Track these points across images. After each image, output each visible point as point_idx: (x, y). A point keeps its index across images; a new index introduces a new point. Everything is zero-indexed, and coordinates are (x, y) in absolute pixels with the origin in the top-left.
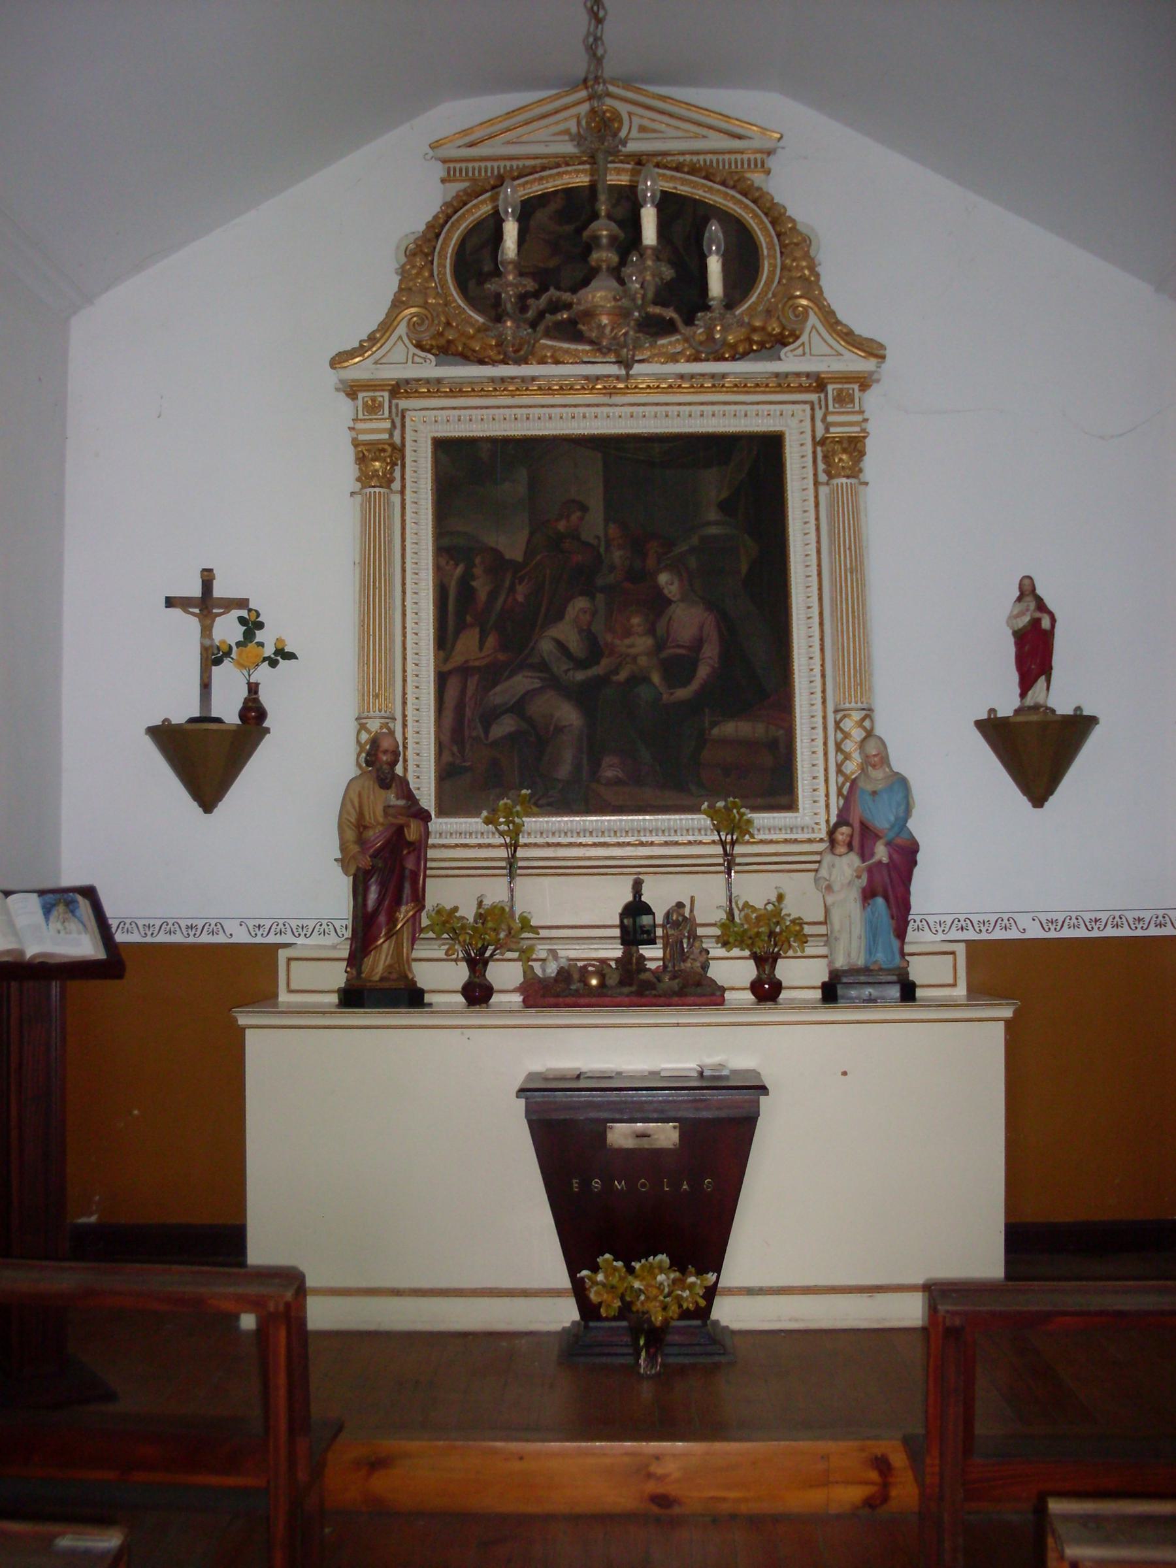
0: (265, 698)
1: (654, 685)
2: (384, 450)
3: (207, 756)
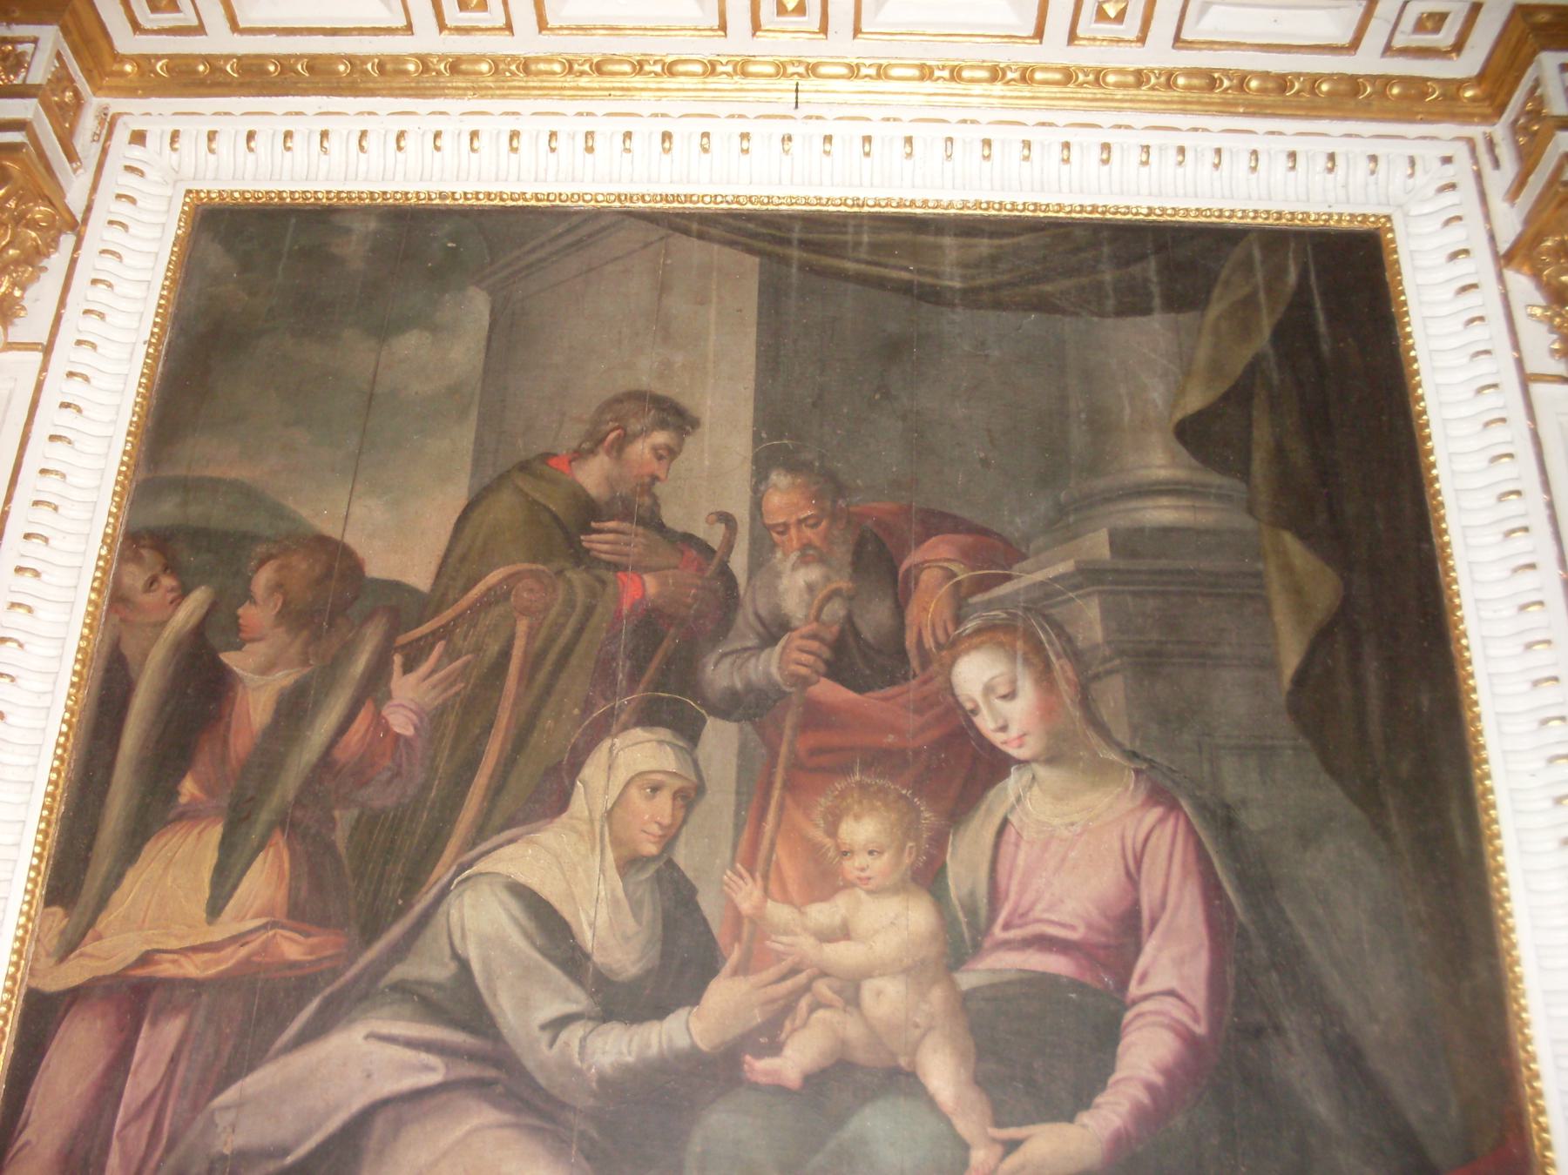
1: (931, 1102)
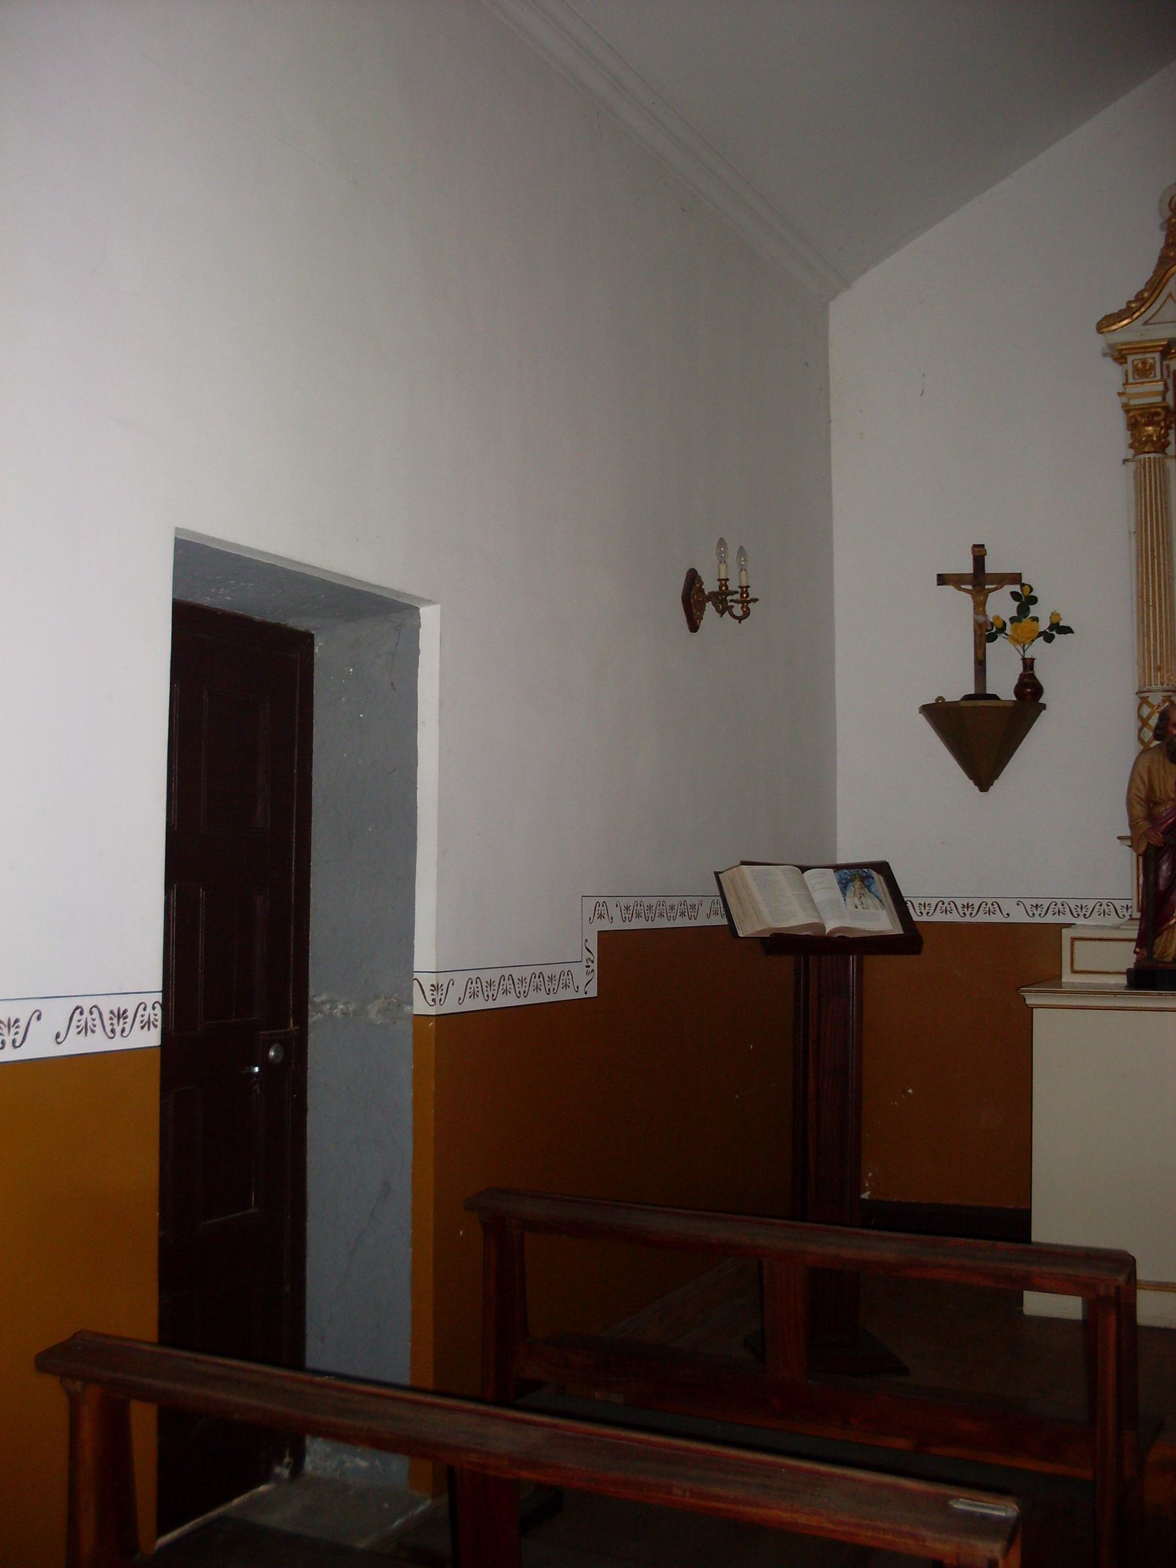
0: (1040, 673)
2: (1157, 414)
3: (983, 733)
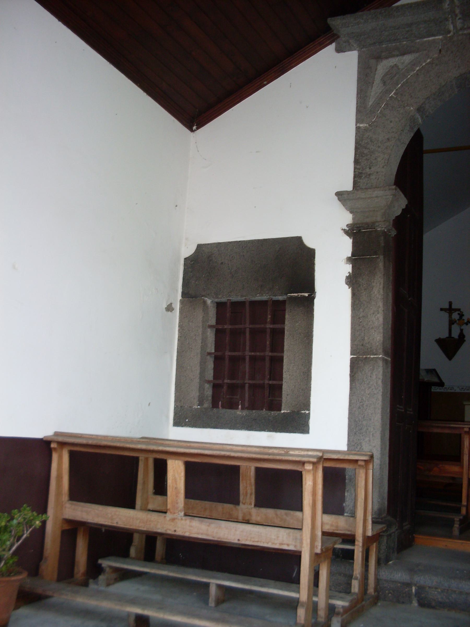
0: (465, 332)
